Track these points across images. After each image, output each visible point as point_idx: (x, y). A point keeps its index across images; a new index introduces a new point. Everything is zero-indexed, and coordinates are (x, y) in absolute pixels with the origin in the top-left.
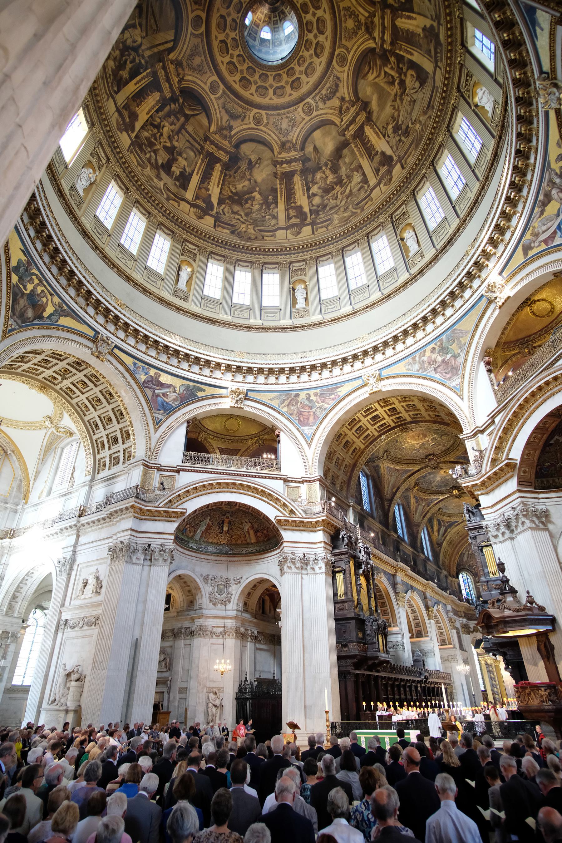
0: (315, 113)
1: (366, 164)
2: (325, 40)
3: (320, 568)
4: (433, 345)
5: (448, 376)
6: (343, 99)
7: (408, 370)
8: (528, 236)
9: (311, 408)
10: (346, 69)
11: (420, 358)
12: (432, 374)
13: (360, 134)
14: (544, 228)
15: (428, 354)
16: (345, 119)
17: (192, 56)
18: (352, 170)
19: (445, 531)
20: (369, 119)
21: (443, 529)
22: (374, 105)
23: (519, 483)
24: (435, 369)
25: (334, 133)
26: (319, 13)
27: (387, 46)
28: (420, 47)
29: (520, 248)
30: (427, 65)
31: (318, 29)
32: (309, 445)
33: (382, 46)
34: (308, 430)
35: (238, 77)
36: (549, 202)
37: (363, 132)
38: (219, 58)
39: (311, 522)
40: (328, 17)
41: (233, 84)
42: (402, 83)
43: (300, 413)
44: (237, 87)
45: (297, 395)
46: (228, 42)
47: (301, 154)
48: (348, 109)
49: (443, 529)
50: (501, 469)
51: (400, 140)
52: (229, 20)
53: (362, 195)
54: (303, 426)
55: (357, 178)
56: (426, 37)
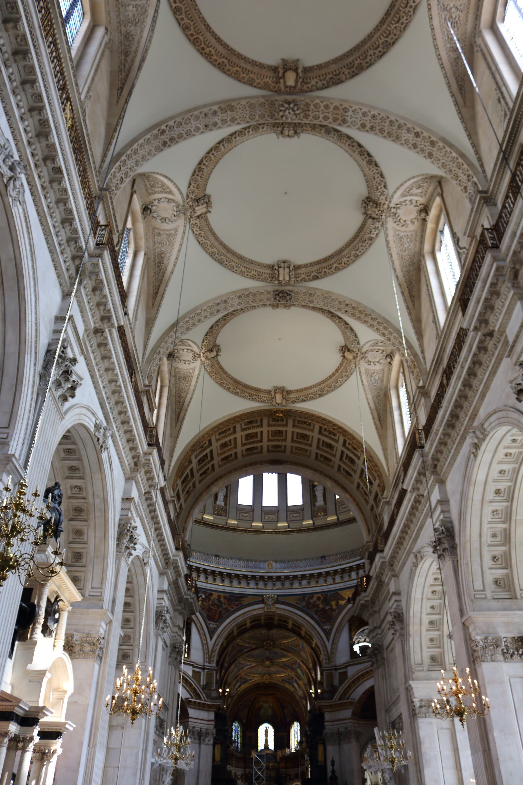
3: (209, 741)
4: (320, 595)
5: (323, 620)
7: (298, 603)
9: (219, 607)
11: (308, 599)
12: (313, 614)
15: (315, 599)
19: (240, 686)
21: (238, 684)
23: (353, 714)
24: (316, 612)
32: (211, 638)
34: (212, 625)
39: (208, 705)
43: (210, 609)
45: (211, 595)
49: (238, 684)
50: (345, 703)
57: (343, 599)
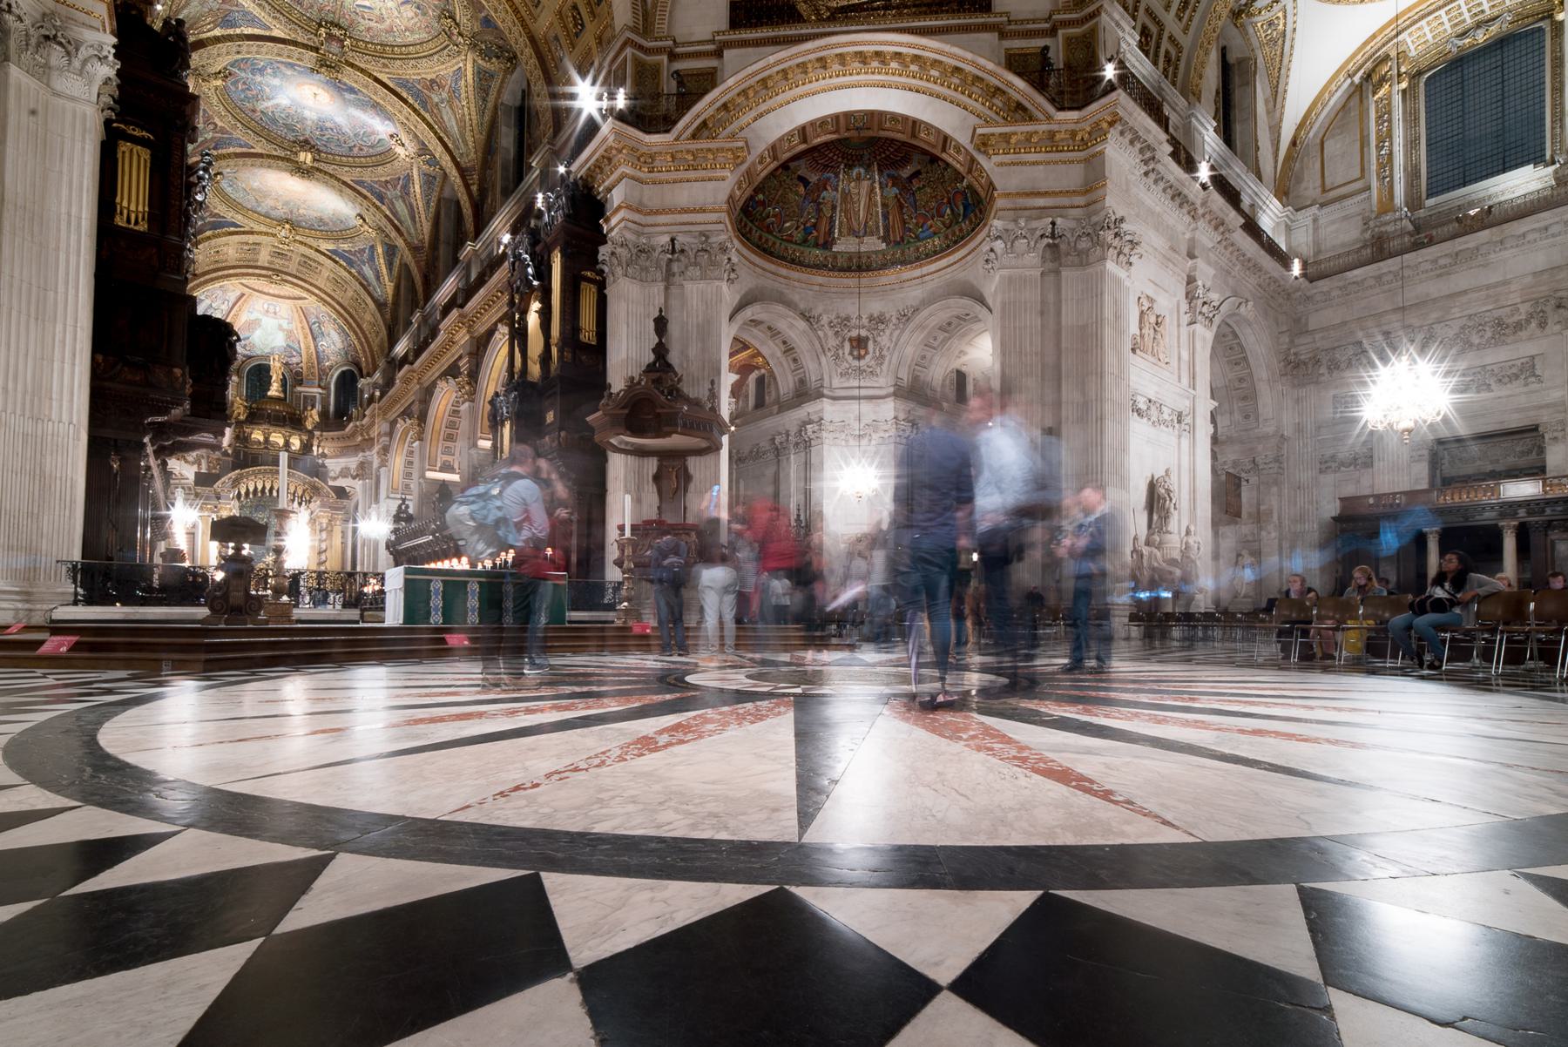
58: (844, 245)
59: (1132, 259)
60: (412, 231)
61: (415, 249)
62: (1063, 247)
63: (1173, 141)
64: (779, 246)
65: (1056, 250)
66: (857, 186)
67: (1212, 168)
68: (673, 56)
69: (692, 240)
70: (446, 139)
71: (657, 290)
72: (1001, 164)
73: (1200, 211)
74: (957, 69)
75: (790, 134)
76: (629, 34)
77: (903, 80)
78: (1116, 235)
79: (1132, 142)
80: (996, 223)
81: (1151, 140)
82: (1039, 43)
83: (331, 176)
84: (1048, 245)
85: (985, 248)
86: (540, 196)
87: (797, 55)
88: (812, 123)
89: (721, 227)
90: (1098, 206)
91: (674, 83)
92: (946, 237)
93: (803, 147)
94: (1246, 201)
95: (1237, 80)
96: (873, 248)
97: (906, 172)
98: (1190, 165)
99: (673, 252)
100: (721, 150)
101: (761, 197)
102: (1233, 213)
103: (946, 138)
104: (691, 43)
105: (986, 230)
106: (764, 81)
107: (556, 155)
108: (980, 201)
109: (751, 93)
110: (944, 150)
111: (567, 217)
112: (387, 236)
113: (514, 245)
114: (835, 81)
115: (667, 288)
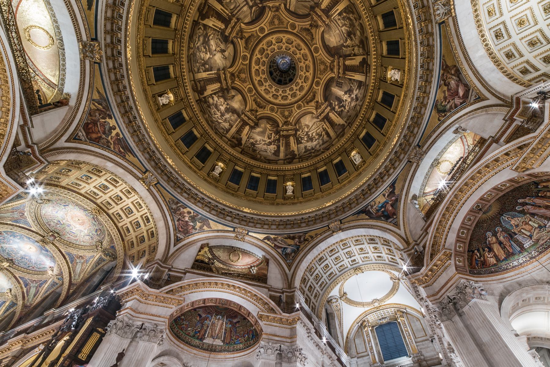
0: (249, 95)
1: (234, 130)
2: (279, 101)
6: (257, 111)
8: (272, 236)
10: (269, 112)
13: (245, 124)
14: (280, 242)
16: (249, 113)
17: (279, 19)
18: (229, 122)
20: (252, 128)
22: (258, 130)
25: (242, 108)
26: (289, 97)
27: (281, 133)
28: (286, 150)
29: (266, 236)
30: (282, 155)
31: (284, 96)
33: (281, 130)
35: (265, 47)
36: (292, 239)
37: (246, 125)
38: (275, 36)
40: (288, 102)
41: (262, 44)
42: (270, 143)
44: (260, 46)
46: (281, 44)
47: (230, 88)
48: (253, 115)
51: (250, 148)
52: (290, 46)
53: (221, 131)
54: (84, 128)
55: (227, 125)
56: (291, 153)
57: (210, 227)
58: (208, 341)
59: (305, 363)
60: (30, 300)
61: (24, 306)
62: (283, 355)
63: (315, 328)
64: (183, 336)
65: (280, 355)
66: (218, 322)
67: (327, 339)
68: (170, 270)
69: (151, 326)
70: (72, 273)
71: (126, 343)
72: (265, 324)
73: (325, 352)
74: (255, 295)
75: (200, 300)
76: (158, 261)
77: (239, 294)
78: (300, 354)
79: (304, 326)
80: (262, 342)
81: (309, 327)
82: (279, 295)
83: (11, 272)
84: (278, 353)
85: (257, 350)
86: (98, 298)
87: (209, 280)
88: (208, 299)
89: (164, 323)
90: (294, 343)
91: (167, 277)
92: (245, 345)
93: (203, 305)
94: (337, 353)
95: (330, 318)
96: (218, 344)
97: (235, 321)
98: (320, 337)
99: (141, 328)
100: (175, 299)
101: (183, 317)
102: (334, 355)
103: (249, 313)
104: (177, 269)
105: (258, 345)
106: (196, 284)
107: (112, 287)
108: (258, 335)
109: (191, 286)
110: (248, 316)
111: (104, 307)
112: (16, 300)
113: (74, 313)
114: (219, 289)
115: (131, 342)
